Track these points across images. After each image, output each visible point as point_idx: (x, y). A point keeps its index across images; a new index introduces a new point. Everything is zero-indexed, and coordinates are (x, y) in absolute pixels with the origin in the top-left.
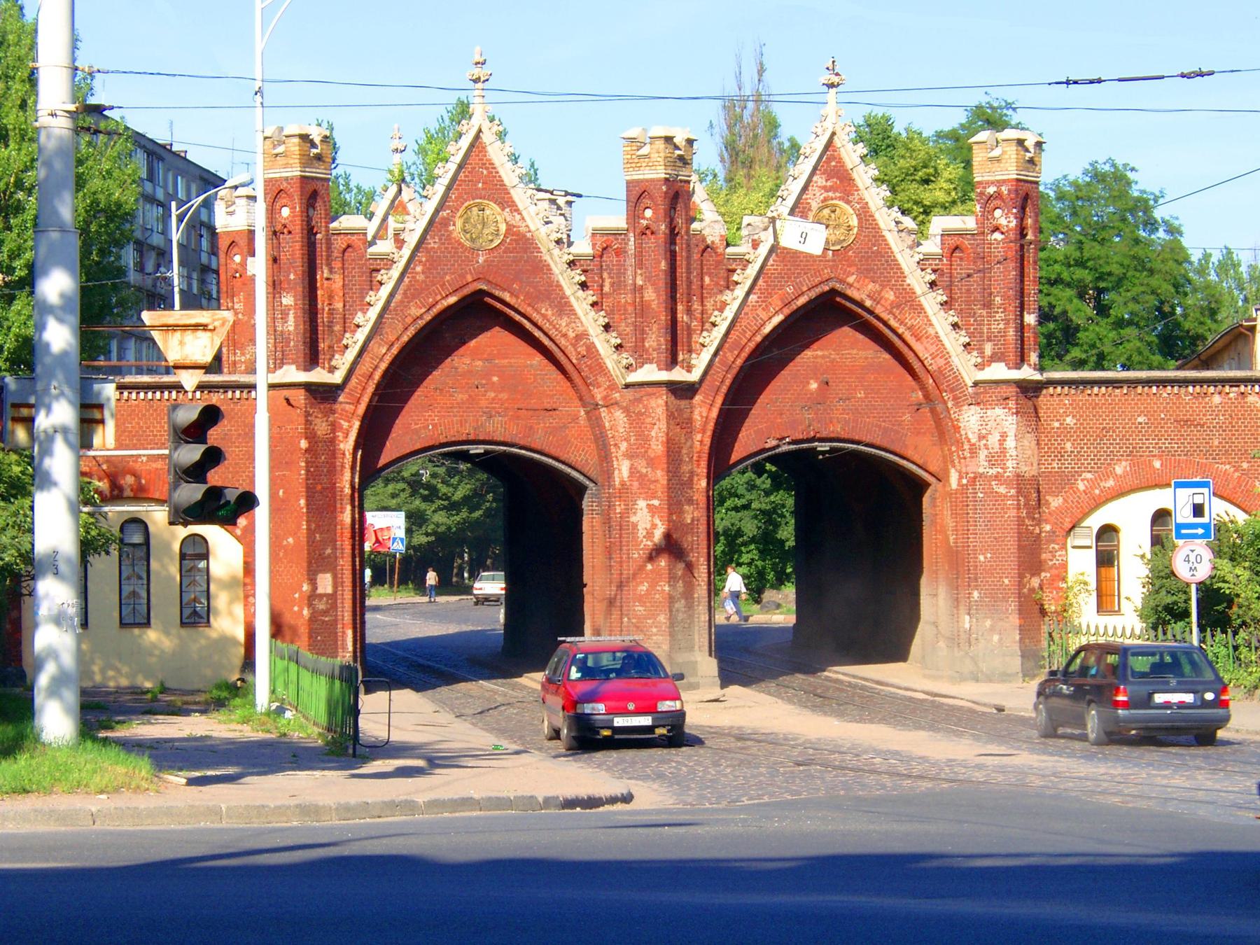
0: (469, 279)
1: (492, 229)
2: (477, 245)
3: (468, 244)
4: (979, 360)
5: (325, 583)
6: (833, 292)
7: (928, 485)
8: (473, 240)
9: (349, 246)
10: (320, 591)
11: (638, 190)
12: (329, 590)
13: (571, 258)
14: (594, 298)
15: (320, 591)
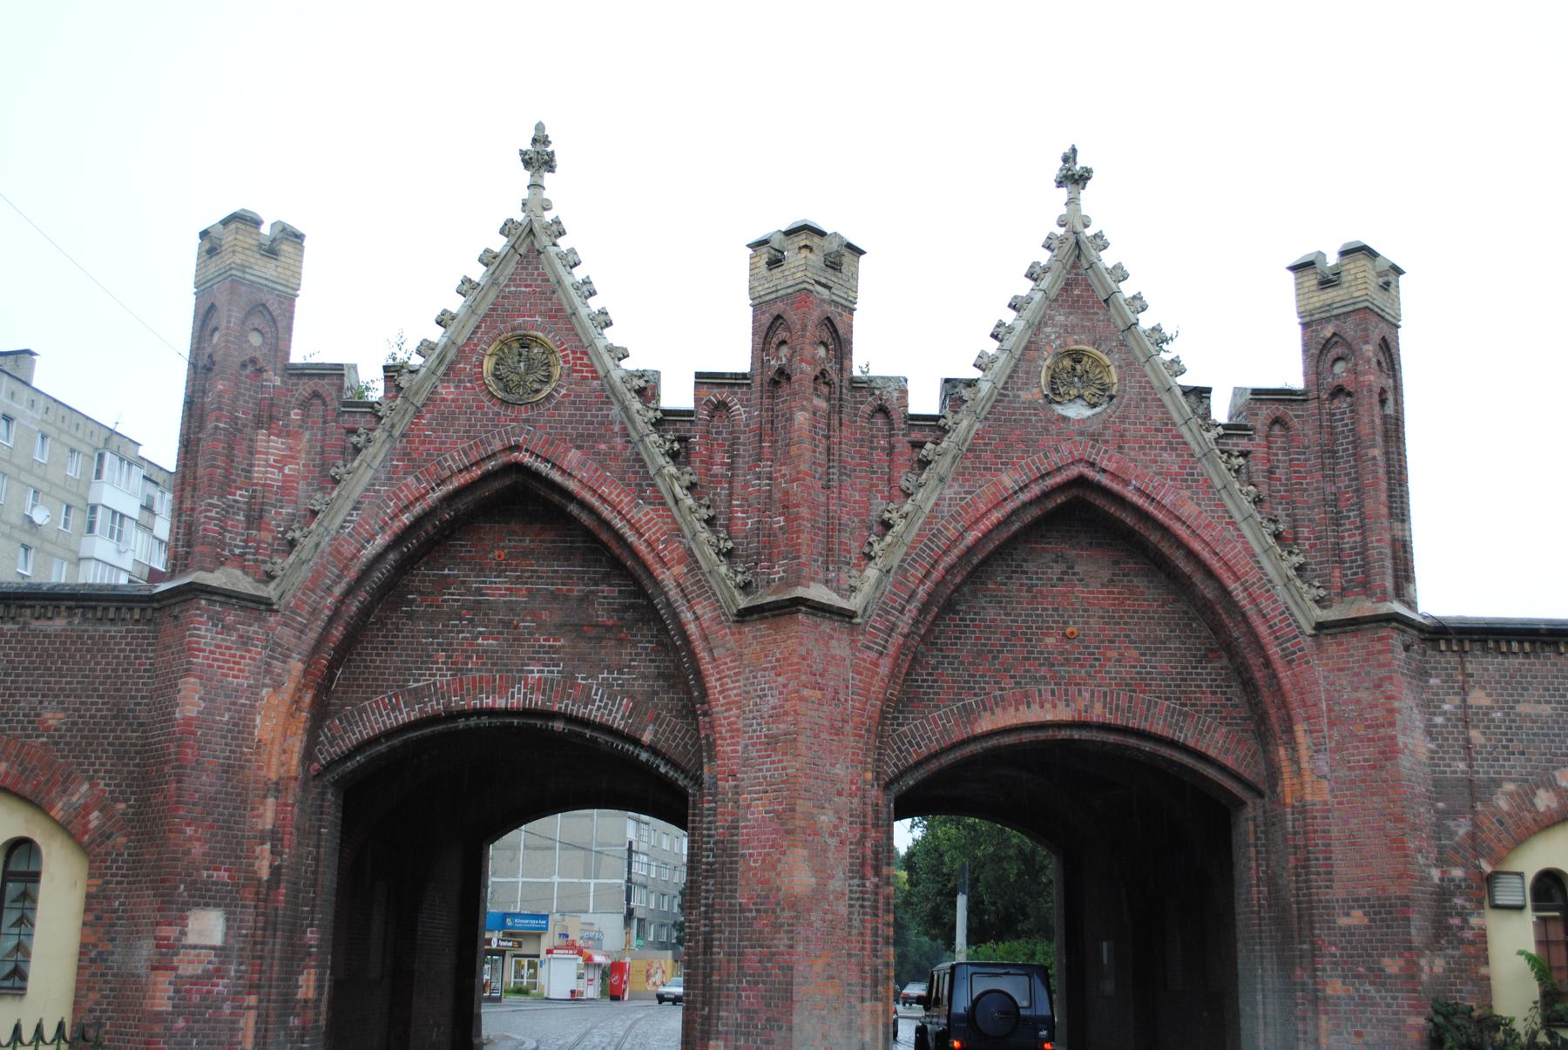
0: (497, 445)
1: (541, 373)
2: (510, 398)
3: (500, 395)
4: (1322, 592)
5: (208, 927)
6: (1081, 481)
7: (1241, 804)
8: (507, 389)
9: (316, 395)
10: (192, 939)
11: (766, 319)
12: (217, 939)
13: (659, 415)
14: (694, 478)
15: (192, 939)
